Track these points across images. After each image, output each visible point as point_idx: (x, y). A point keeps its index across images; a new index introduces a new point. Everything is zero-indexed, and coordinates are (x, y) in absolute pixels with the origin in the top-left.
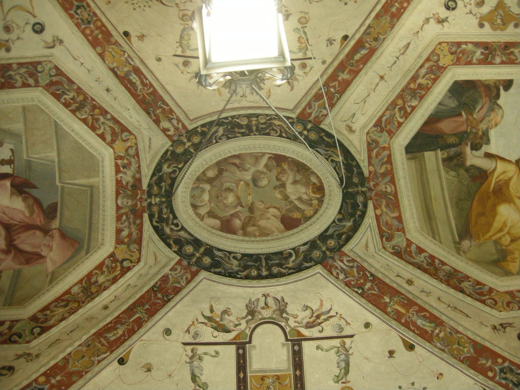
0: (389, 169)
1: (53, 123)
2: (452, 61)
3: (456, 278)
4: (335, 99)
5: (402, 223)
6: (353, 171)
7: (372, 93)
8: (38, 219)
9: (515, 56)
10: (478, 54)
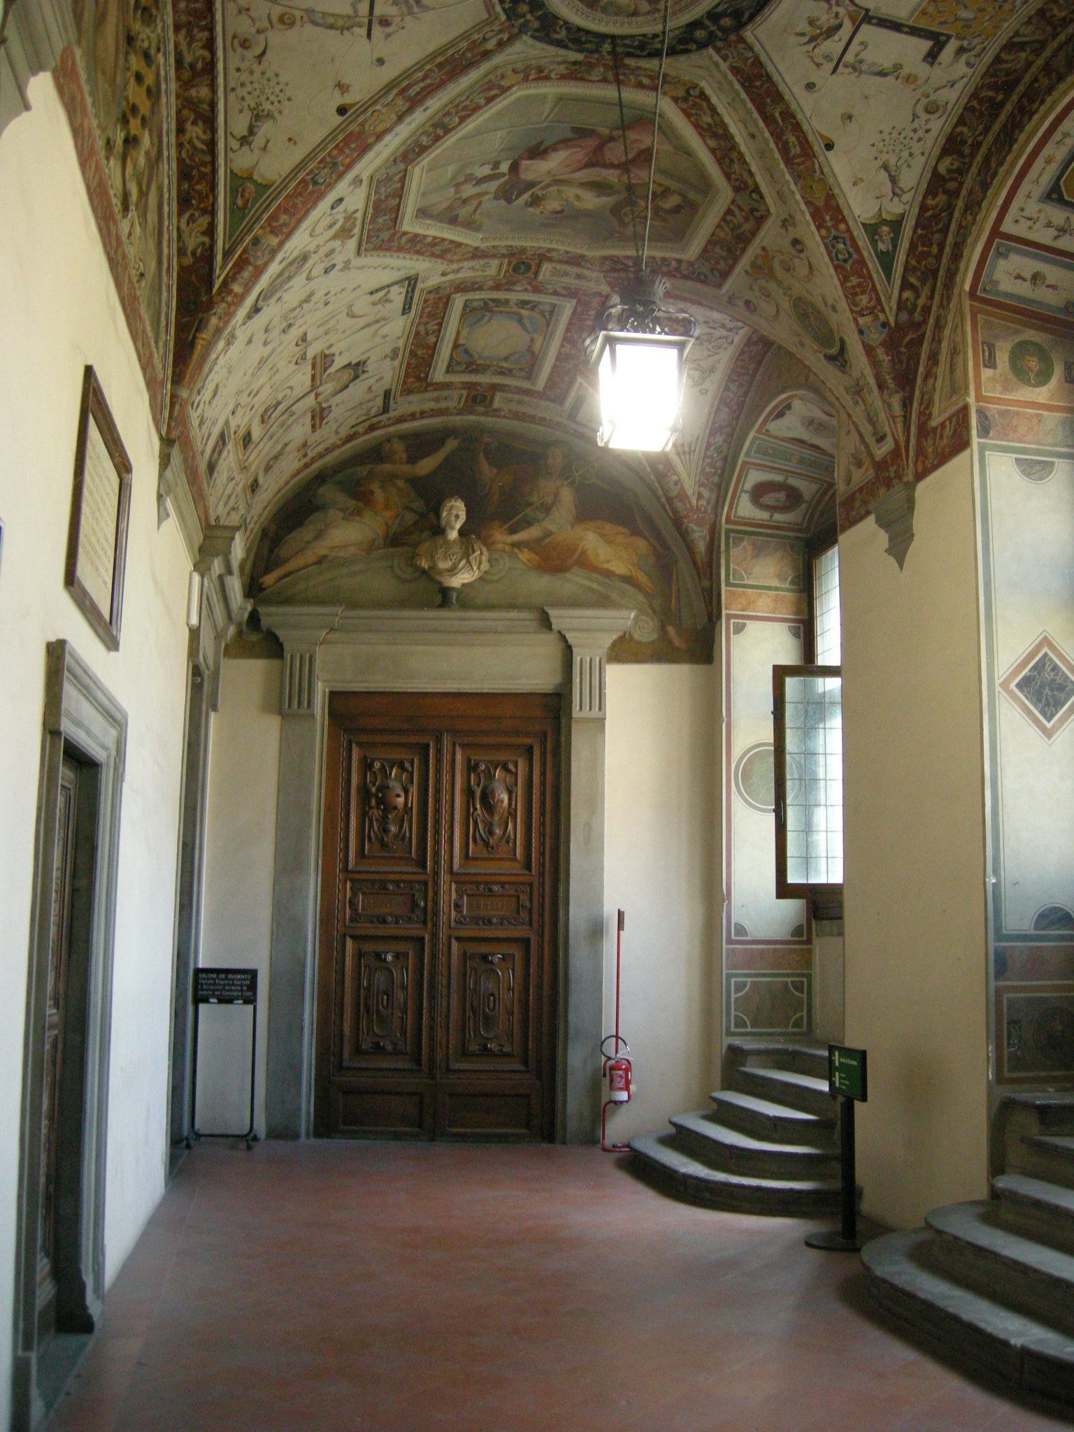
8: (592, 143)
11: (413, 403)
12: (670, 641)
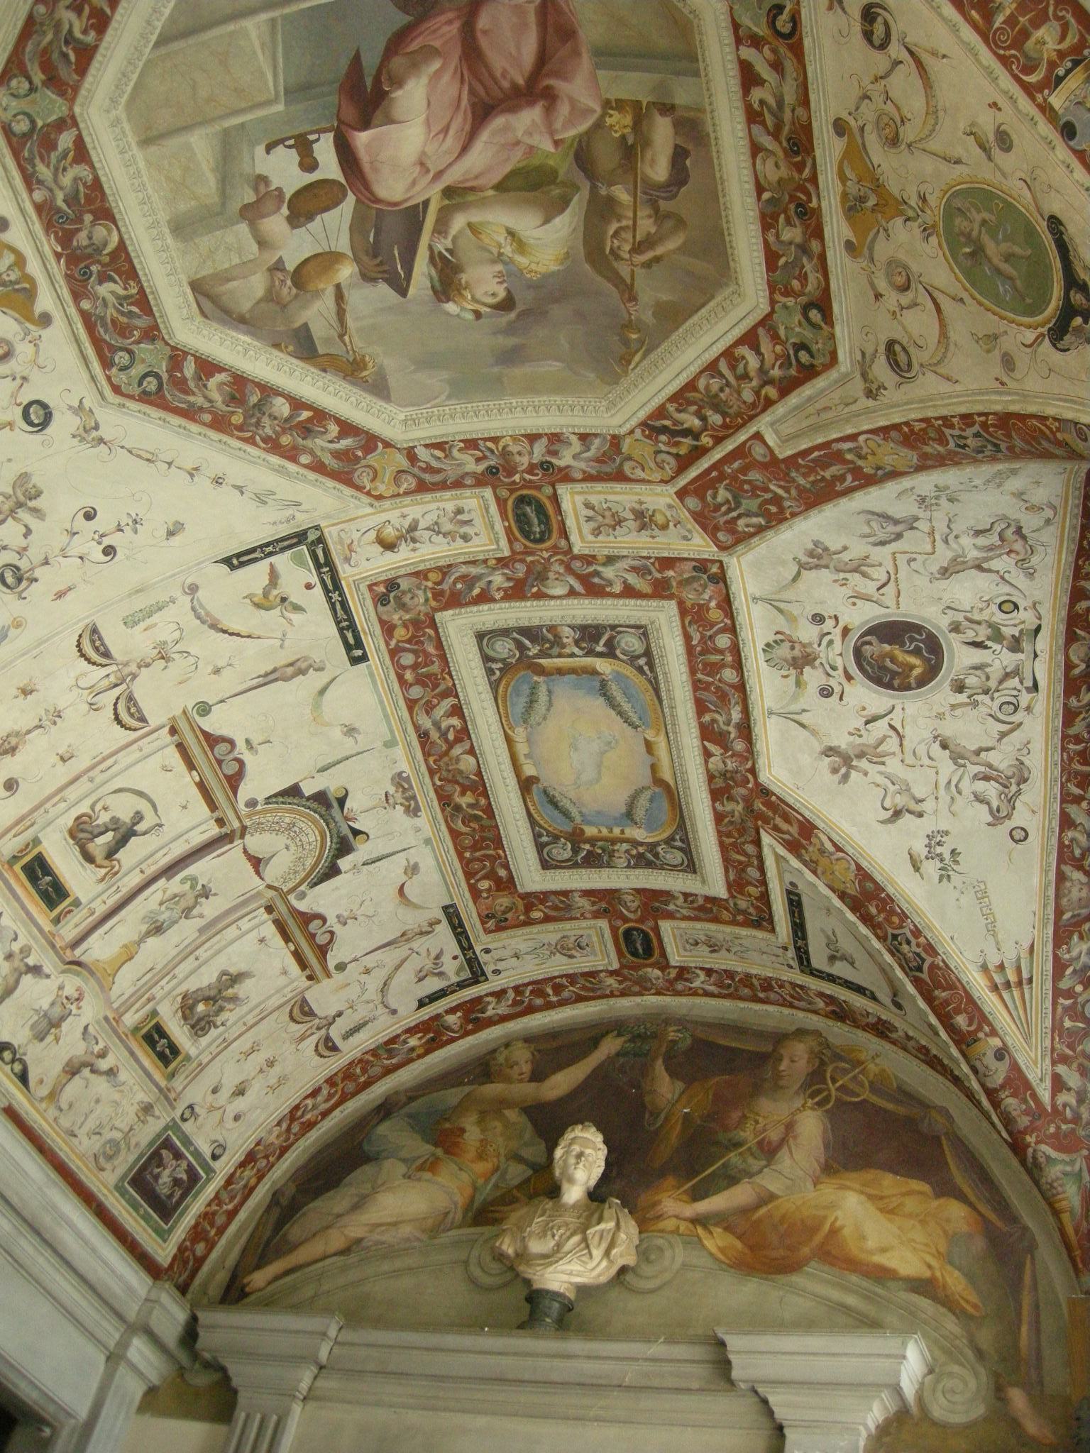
1: (163, 50)
11: (518, 958)
12: (1015, 1424)
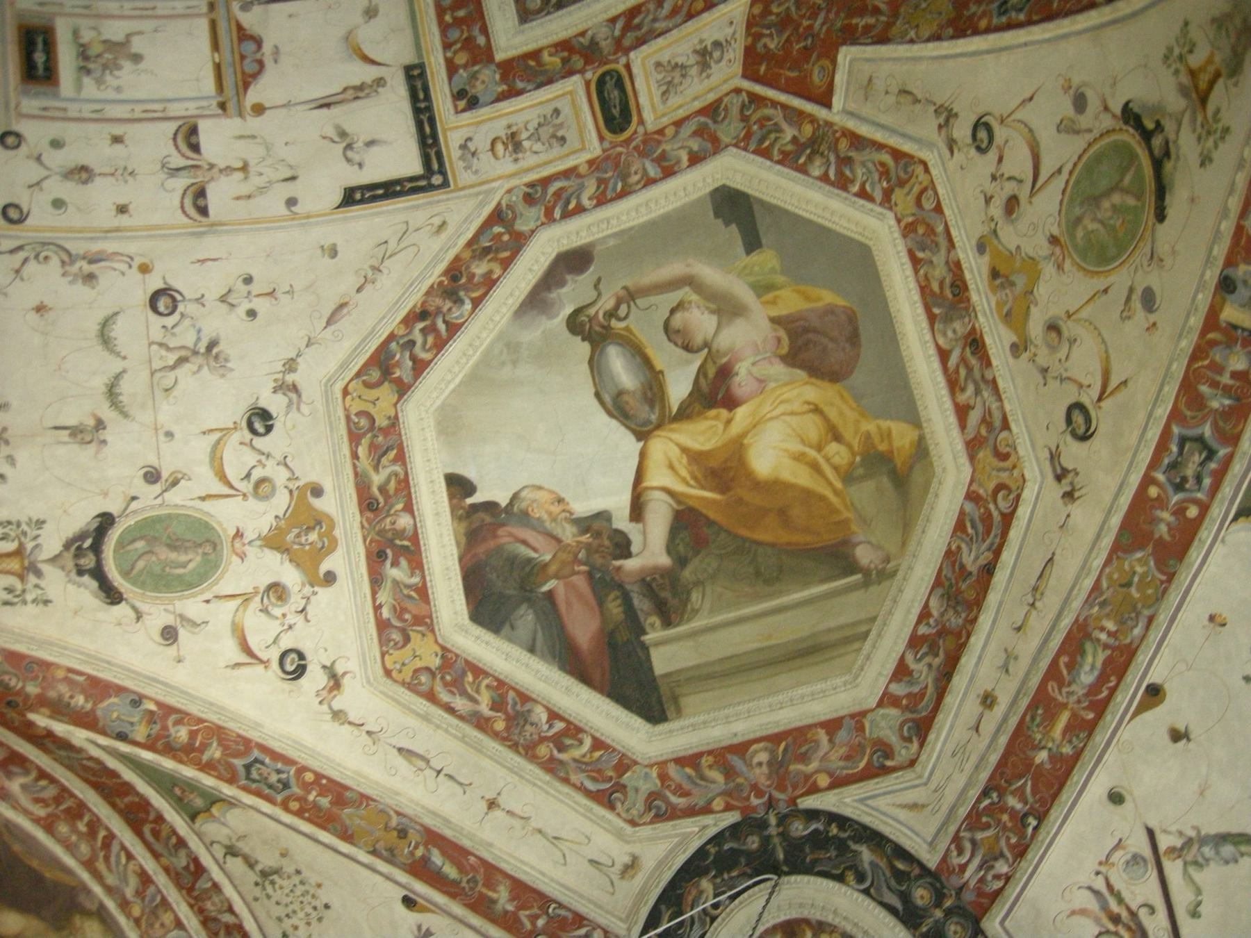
0: (711, 759)
2: (424, 635)
3: (957, 583)
4: (562, 912)
5: (842, 718)
6: (731, 849)
7: (534, 824)
9: (388, 481)
10: (397, 573)
